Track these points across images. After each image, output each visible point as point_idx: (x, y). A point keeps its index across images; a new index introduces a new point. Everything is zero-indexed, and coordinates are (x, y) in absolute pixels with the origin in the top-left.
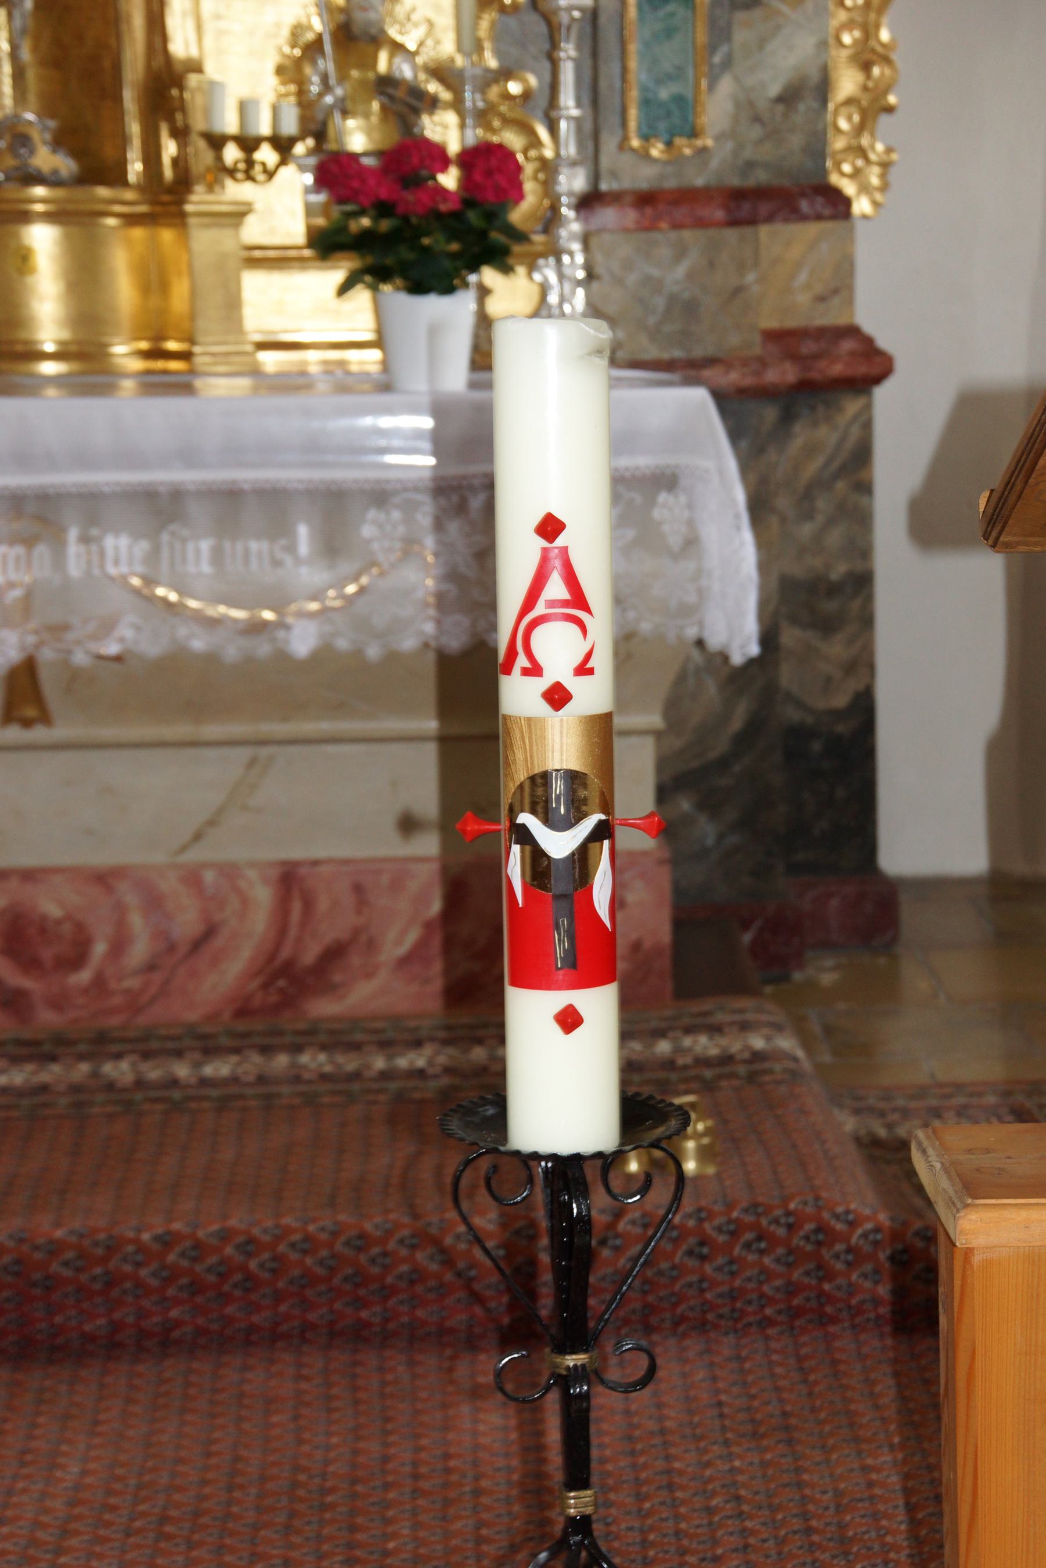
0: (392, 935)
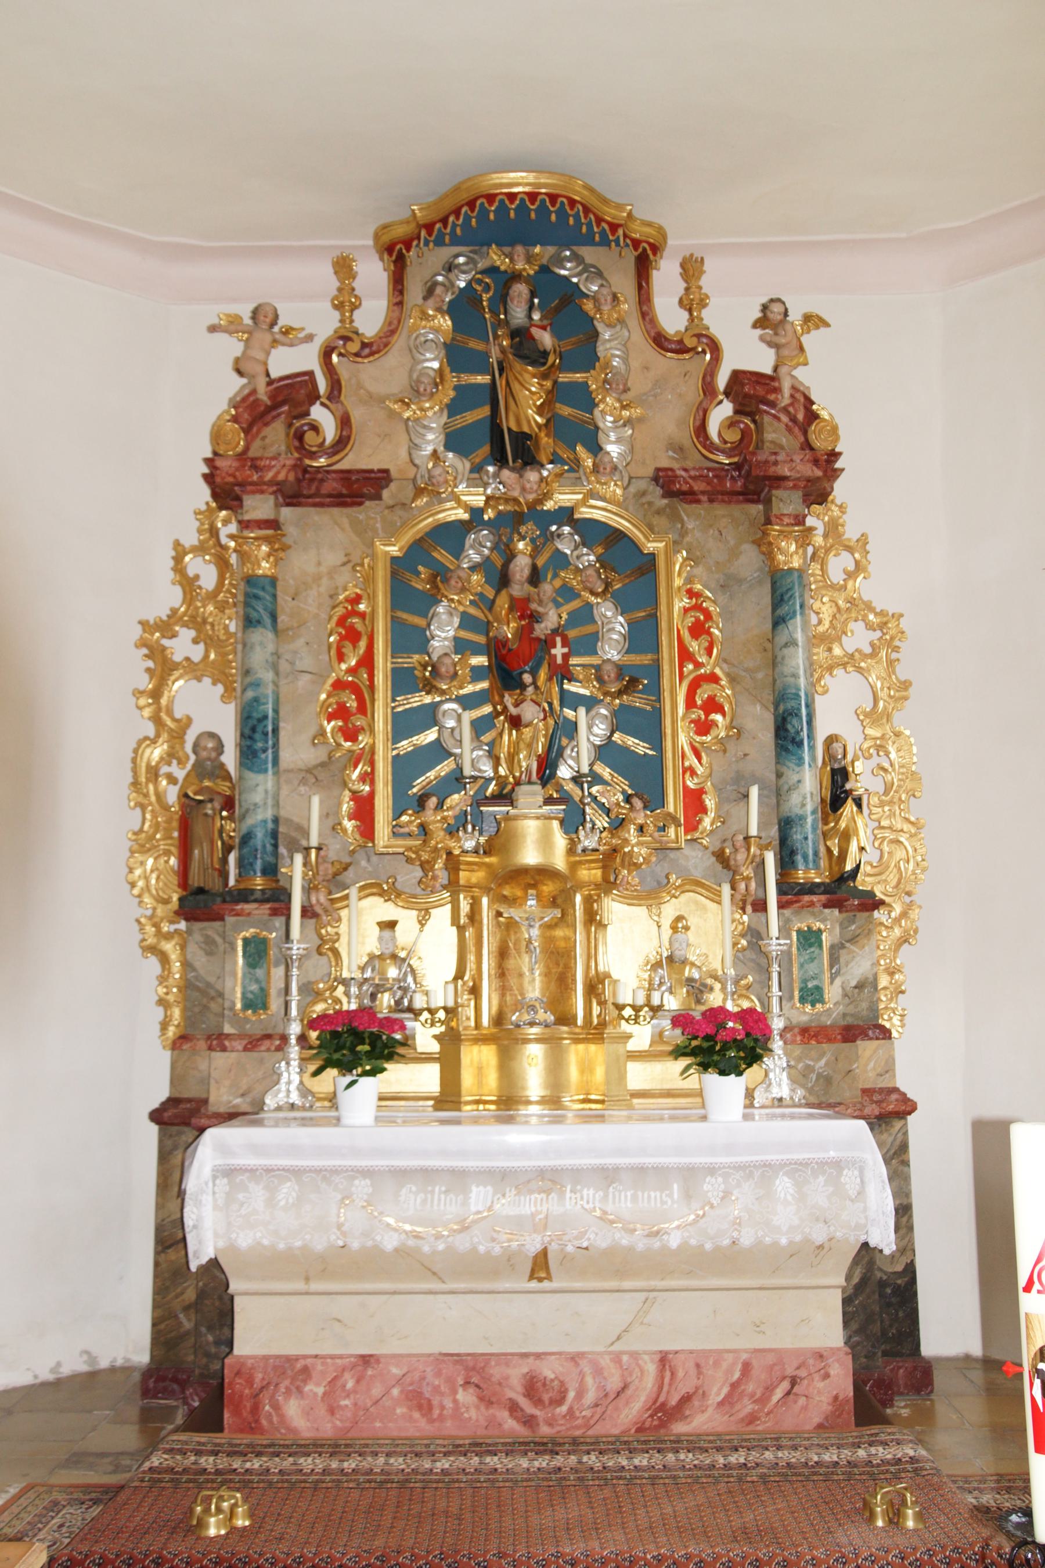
0: (715, 1390)
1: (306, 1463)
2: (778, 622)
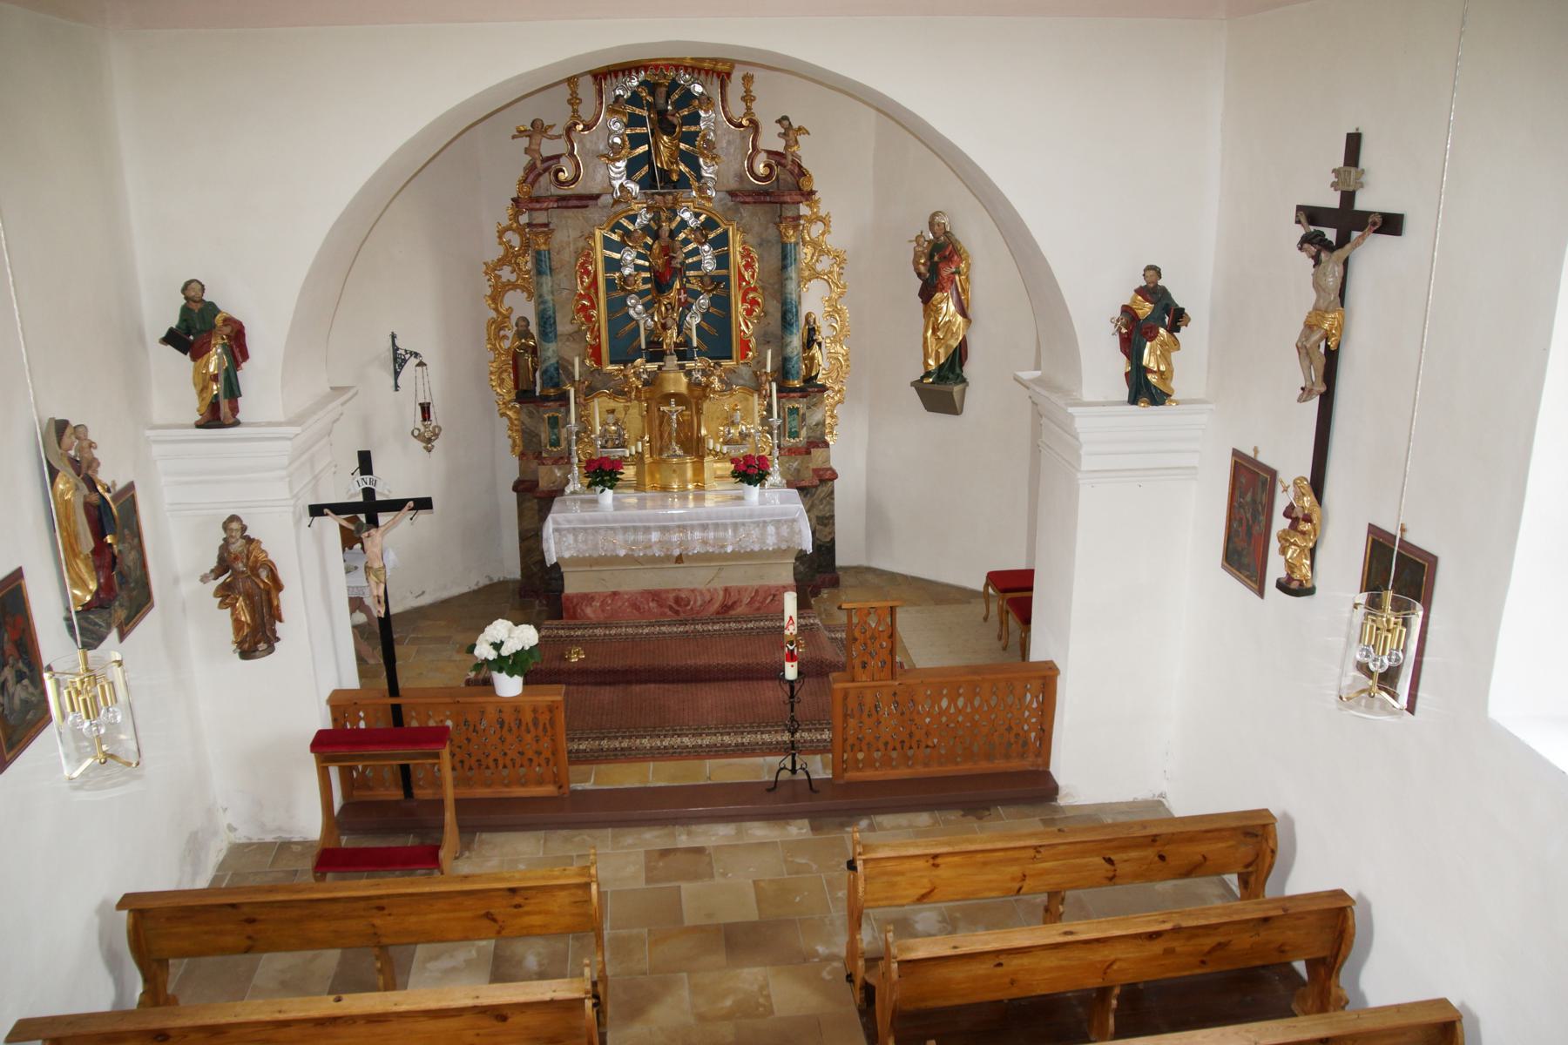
1: (598, 631)
2: (784, 267)
